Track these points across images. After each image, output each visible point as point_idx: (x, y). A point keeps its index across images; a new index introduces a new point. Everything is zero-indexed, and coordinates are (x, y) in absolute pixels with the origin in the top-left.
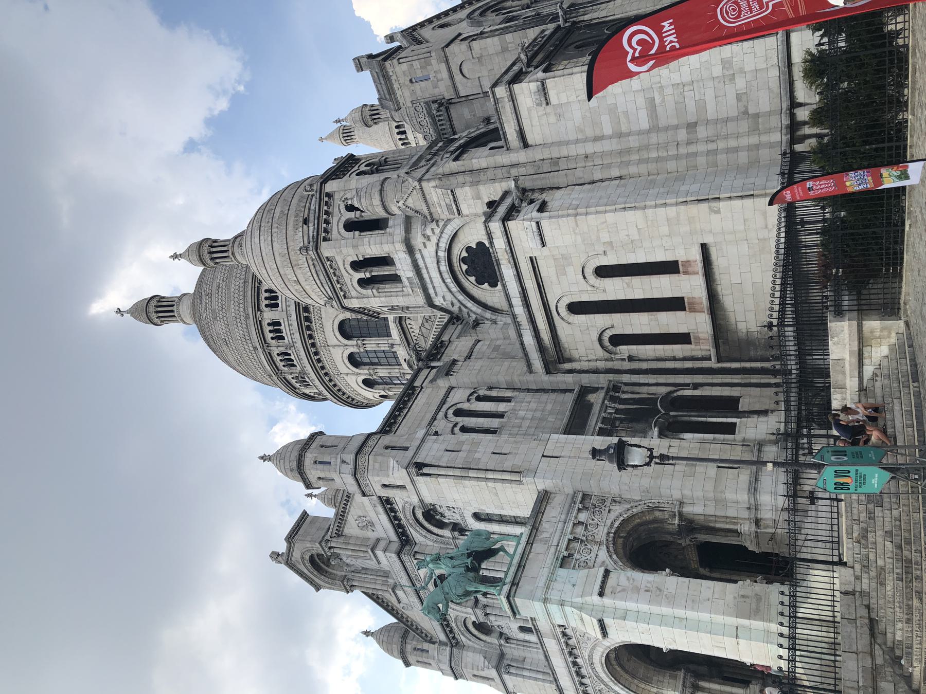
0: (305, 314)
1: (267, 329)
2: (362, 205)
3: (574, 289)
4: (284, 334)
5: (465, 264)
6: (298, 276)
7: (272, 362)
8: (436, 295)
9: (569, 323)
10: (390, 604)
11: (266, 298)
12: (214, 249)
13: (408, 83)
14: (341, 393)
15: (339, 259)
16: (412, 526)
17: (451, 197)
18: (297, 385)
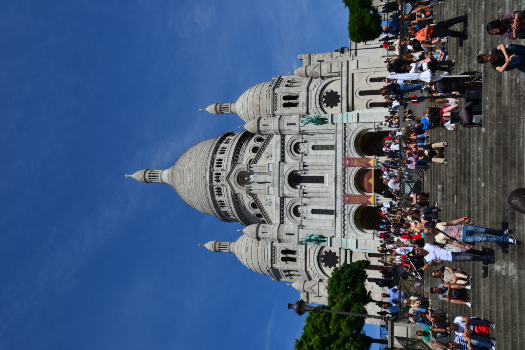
3: (363, 86)
4: (222, 165)
5: (324, 98)
6: (260, 103)
8: (311, 109)
9: (358, 98)
11: (220, 150)
12: (222, 105)
13: (316, 62)
15: (279, 95)
16: (288, 152)
17: (330, 66)
18: (216, 193)
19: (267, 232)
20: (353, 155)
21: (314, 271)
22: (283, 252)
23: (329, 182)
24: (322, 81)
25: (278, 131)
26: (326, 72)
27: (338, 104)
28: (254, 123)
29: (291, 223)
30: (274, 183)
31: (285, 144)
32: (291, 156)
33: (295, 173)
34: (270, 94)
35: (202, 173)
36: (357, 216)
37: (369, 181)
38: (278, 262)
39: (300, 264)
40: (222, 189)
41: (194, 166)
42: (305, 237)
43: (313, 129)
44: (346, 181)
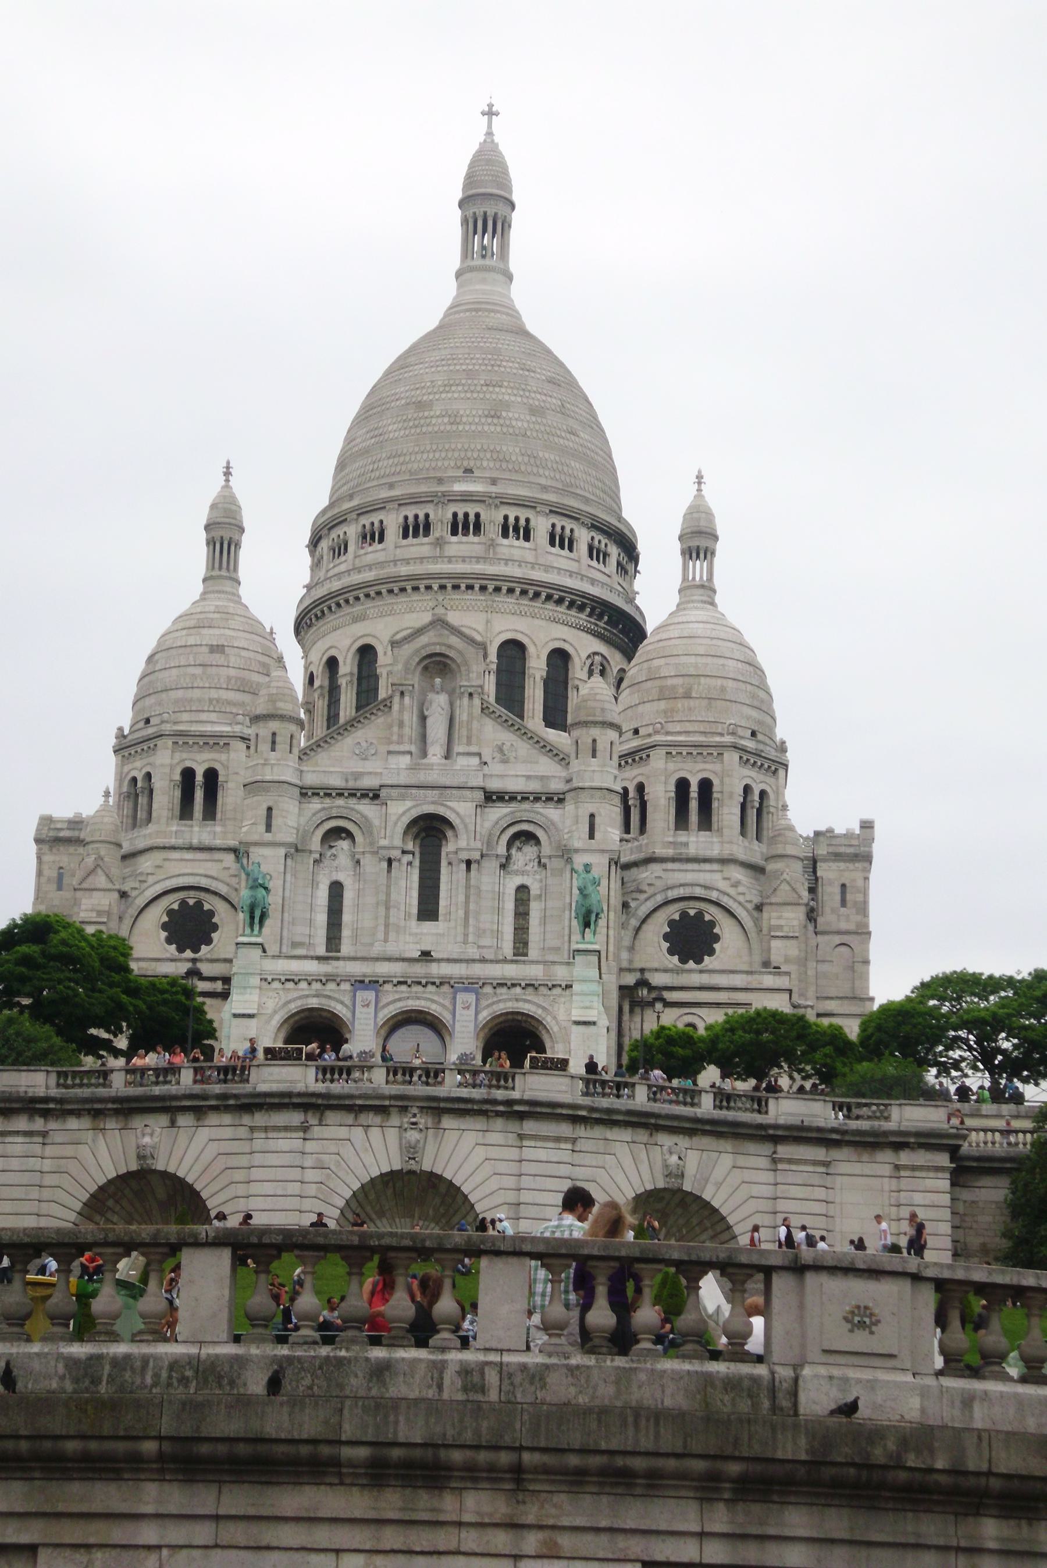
0: (543, 596)
1: (523, 514)
2: (785, 829)
4: (511, 541)
6: (697, 702)
7: (467, 498)
8: (664, 870)
10: (360, 725)
11: (563, 528)
12: (709, 556)
13: (843, 881)
14: (396, 590)
15: (717, 767)
16: (514, 812)
17: (791, 935)
19: (277, 747)
20: (484, 1008)
21: (152, 874)
22: (211, 776)
23: (422, 934)
24: (750, 906)
25: (575, 783)
26: (773, 922)
27: (677, 957)
28: (603, 710)
29: (303, 821)
30: (422, 772)
31: (538, 805)
33: (449, 834)
34: (722, 735)
35: (485, 464)
36: (321, 1016)
38: (178, 756)
39: (174, 828)
40: (426, 540)
41: (511, 430)
42: (264, 868)
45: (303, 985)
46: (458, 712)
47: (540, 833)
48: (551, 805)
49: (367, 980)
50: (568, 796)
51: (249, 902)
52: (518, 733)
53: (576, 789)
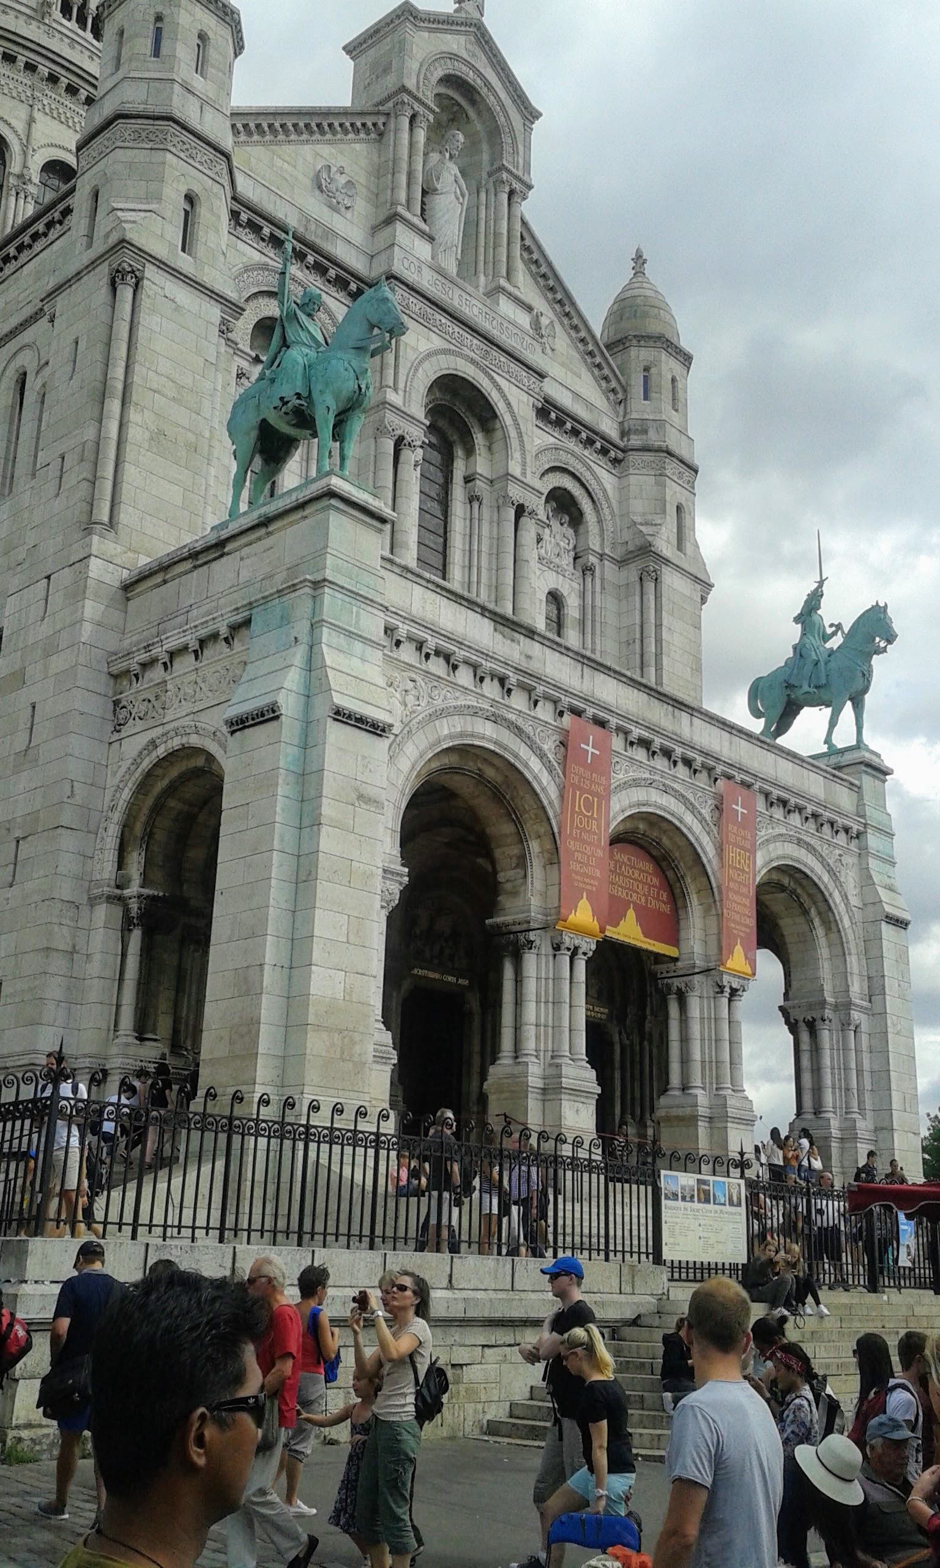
25: (653, 438)
30: (459, 292)
32: (543, 458)
33: (479, 438)
37: (631, 914)
43: (665, 635)
44: (660, 763)
45: (464, 676)
46: (483, 215)
47: (586, 505)
48: (602, 461)
49: (591, 711)
50: (632, 457)
51: (352, 385)
52: (557, 307)
53: (659, 450)
